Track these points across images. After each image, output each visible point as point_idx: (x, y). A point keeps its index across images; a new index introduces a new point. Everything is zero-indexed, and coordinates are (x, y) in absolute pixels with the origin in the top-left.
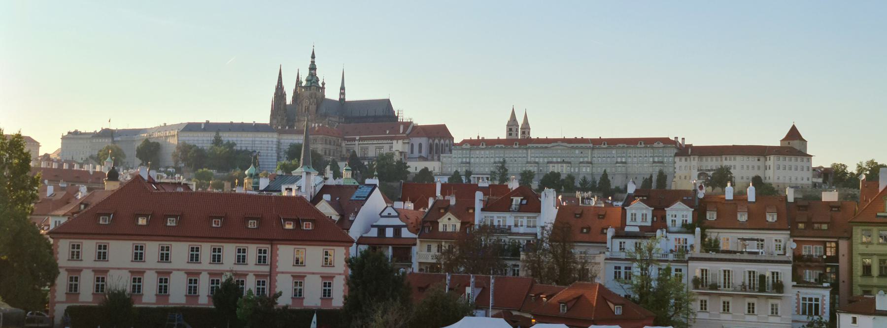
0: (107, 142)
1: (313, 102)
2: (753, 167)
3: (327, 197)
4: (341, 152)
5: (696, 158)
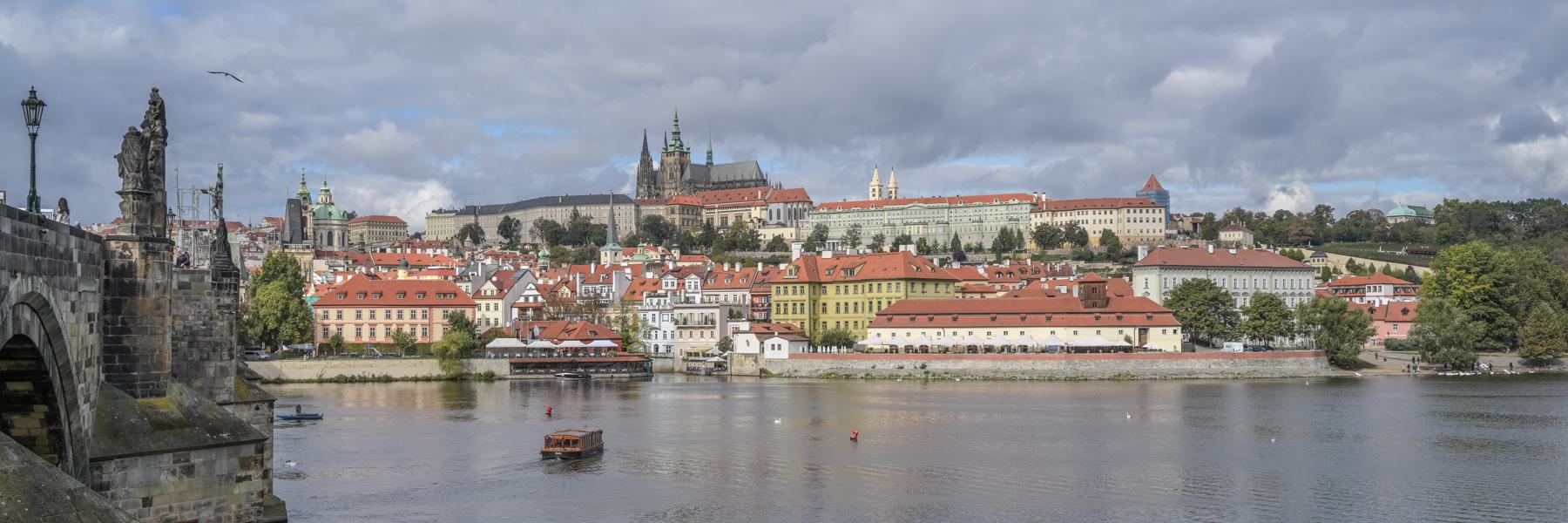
0: (471, 220)
2: (1105, 221)
3: (494, 279)
4: (701, 221)
5: (1050, 213)
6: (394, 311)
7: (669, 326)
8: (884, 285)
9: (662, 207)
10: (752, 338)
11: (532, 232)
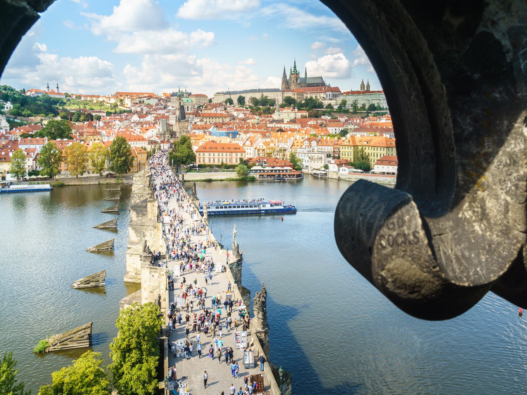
0: (228, 97)
6: (221, 154)
7: (307, 159)
8: (379, 149)
9: (291, 93)
10: (335, 166)
11: (248, 101)
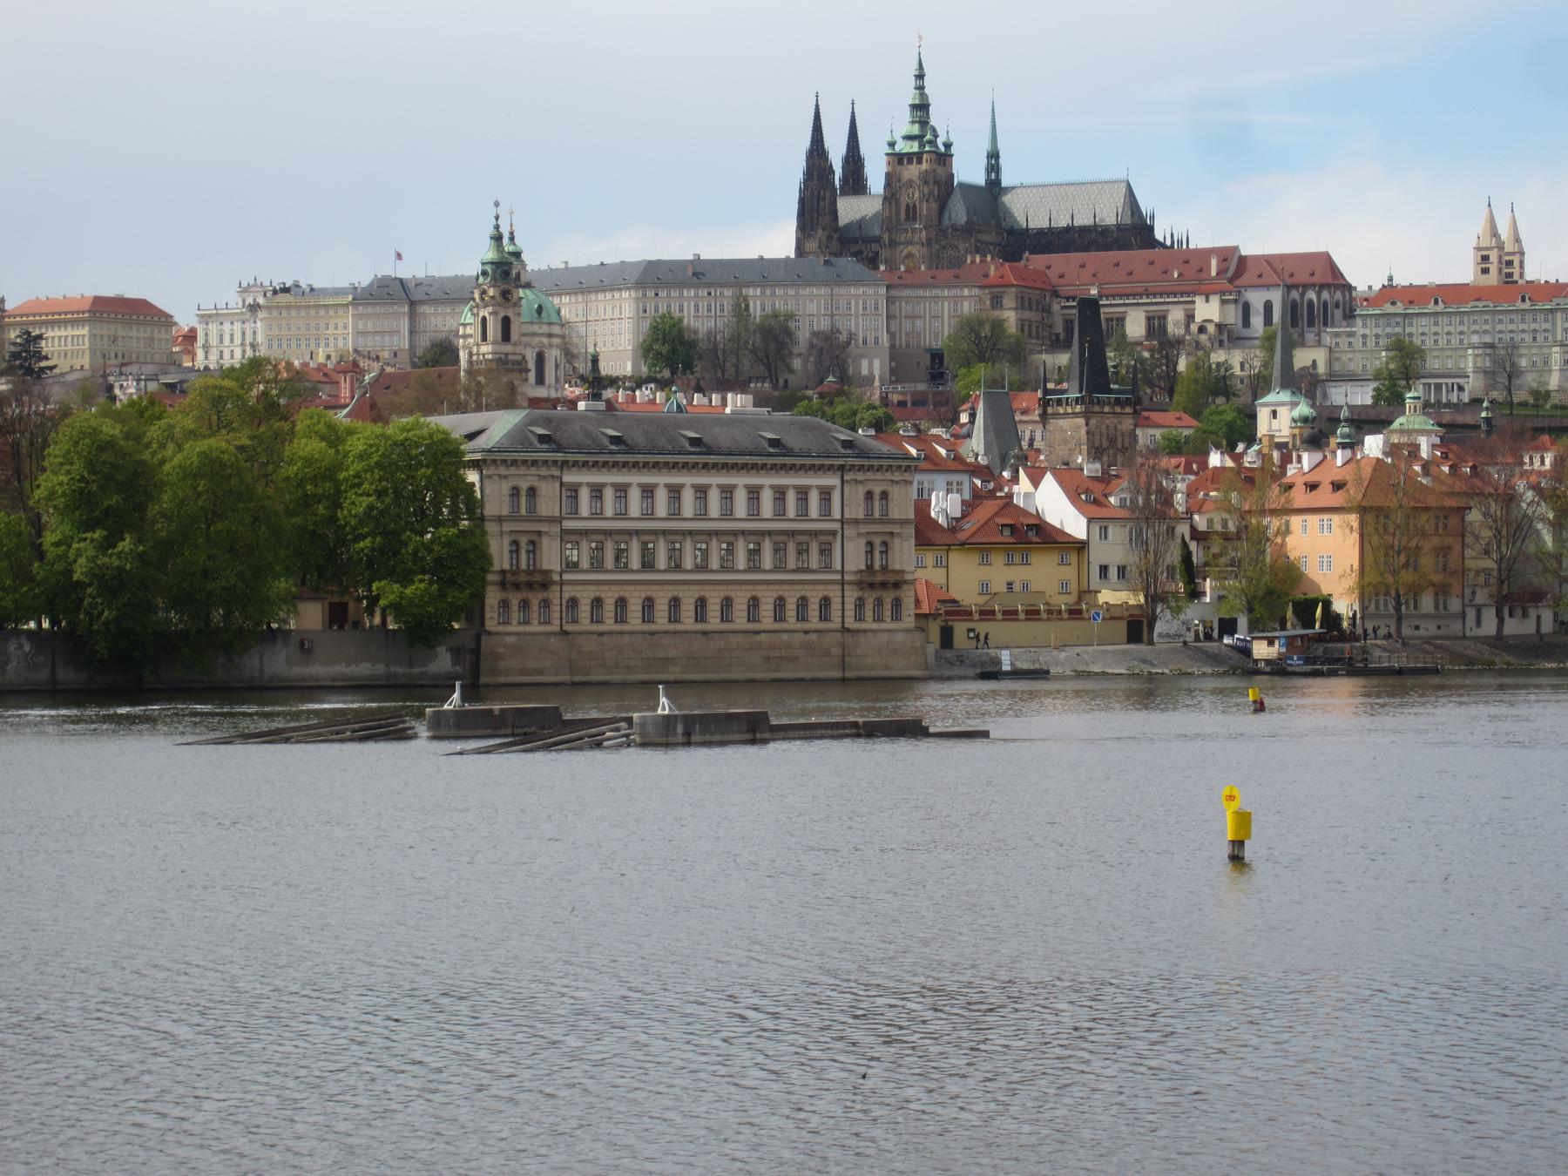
1: (931, 193)
